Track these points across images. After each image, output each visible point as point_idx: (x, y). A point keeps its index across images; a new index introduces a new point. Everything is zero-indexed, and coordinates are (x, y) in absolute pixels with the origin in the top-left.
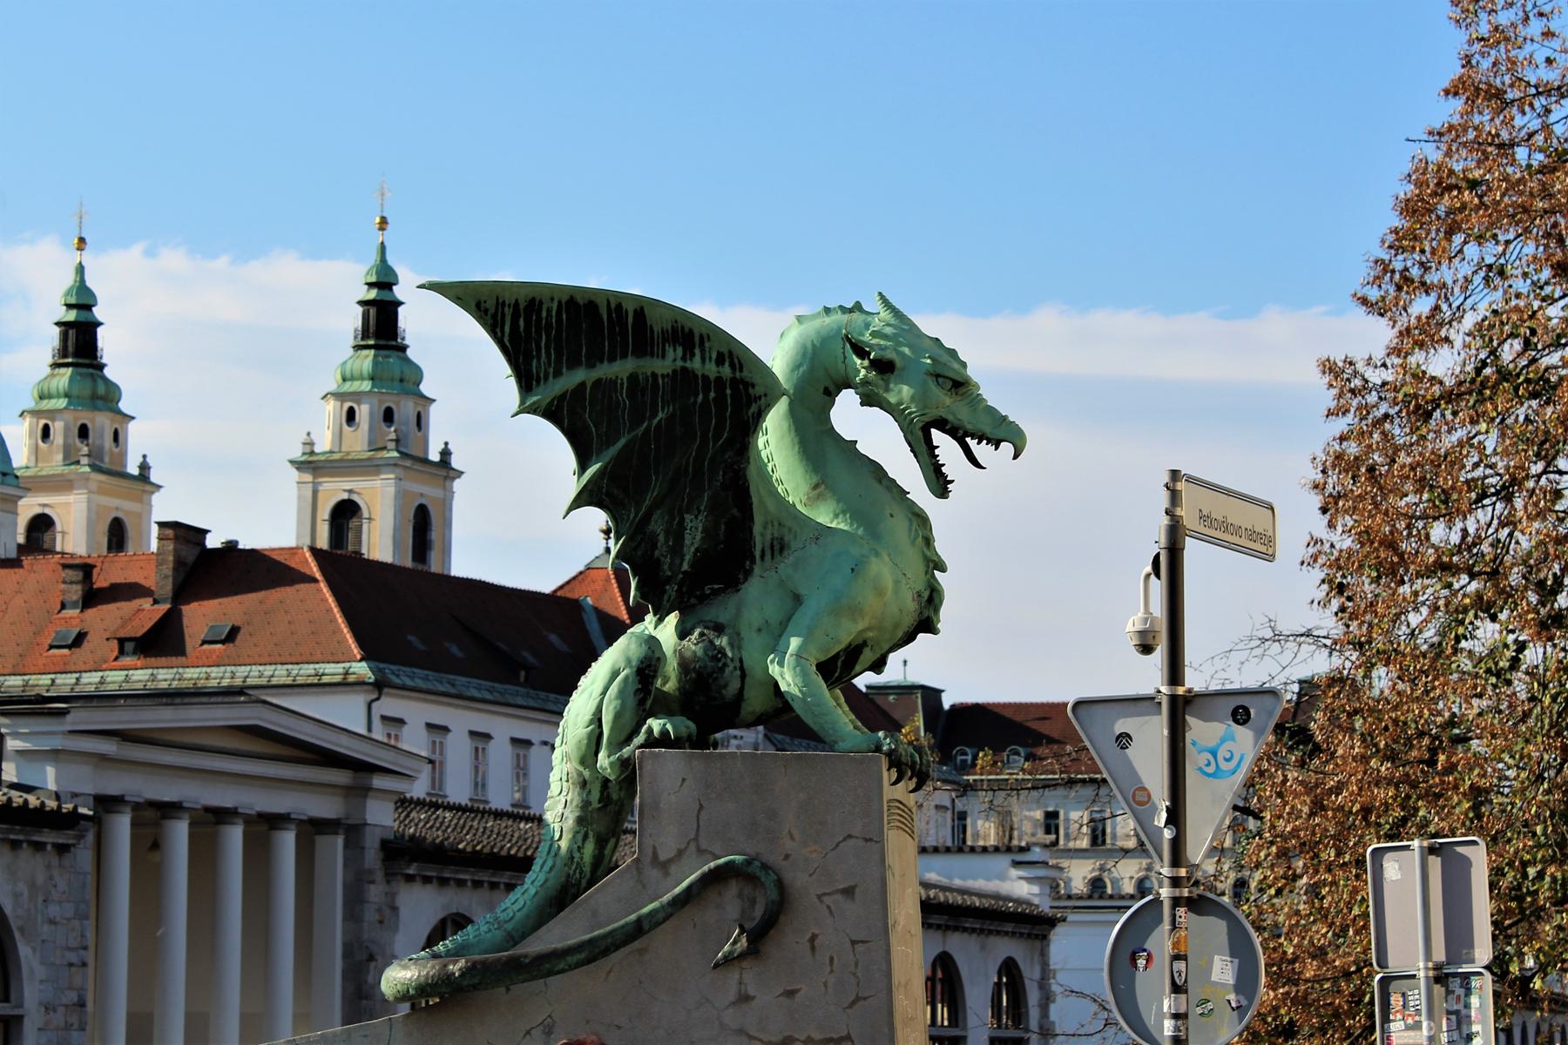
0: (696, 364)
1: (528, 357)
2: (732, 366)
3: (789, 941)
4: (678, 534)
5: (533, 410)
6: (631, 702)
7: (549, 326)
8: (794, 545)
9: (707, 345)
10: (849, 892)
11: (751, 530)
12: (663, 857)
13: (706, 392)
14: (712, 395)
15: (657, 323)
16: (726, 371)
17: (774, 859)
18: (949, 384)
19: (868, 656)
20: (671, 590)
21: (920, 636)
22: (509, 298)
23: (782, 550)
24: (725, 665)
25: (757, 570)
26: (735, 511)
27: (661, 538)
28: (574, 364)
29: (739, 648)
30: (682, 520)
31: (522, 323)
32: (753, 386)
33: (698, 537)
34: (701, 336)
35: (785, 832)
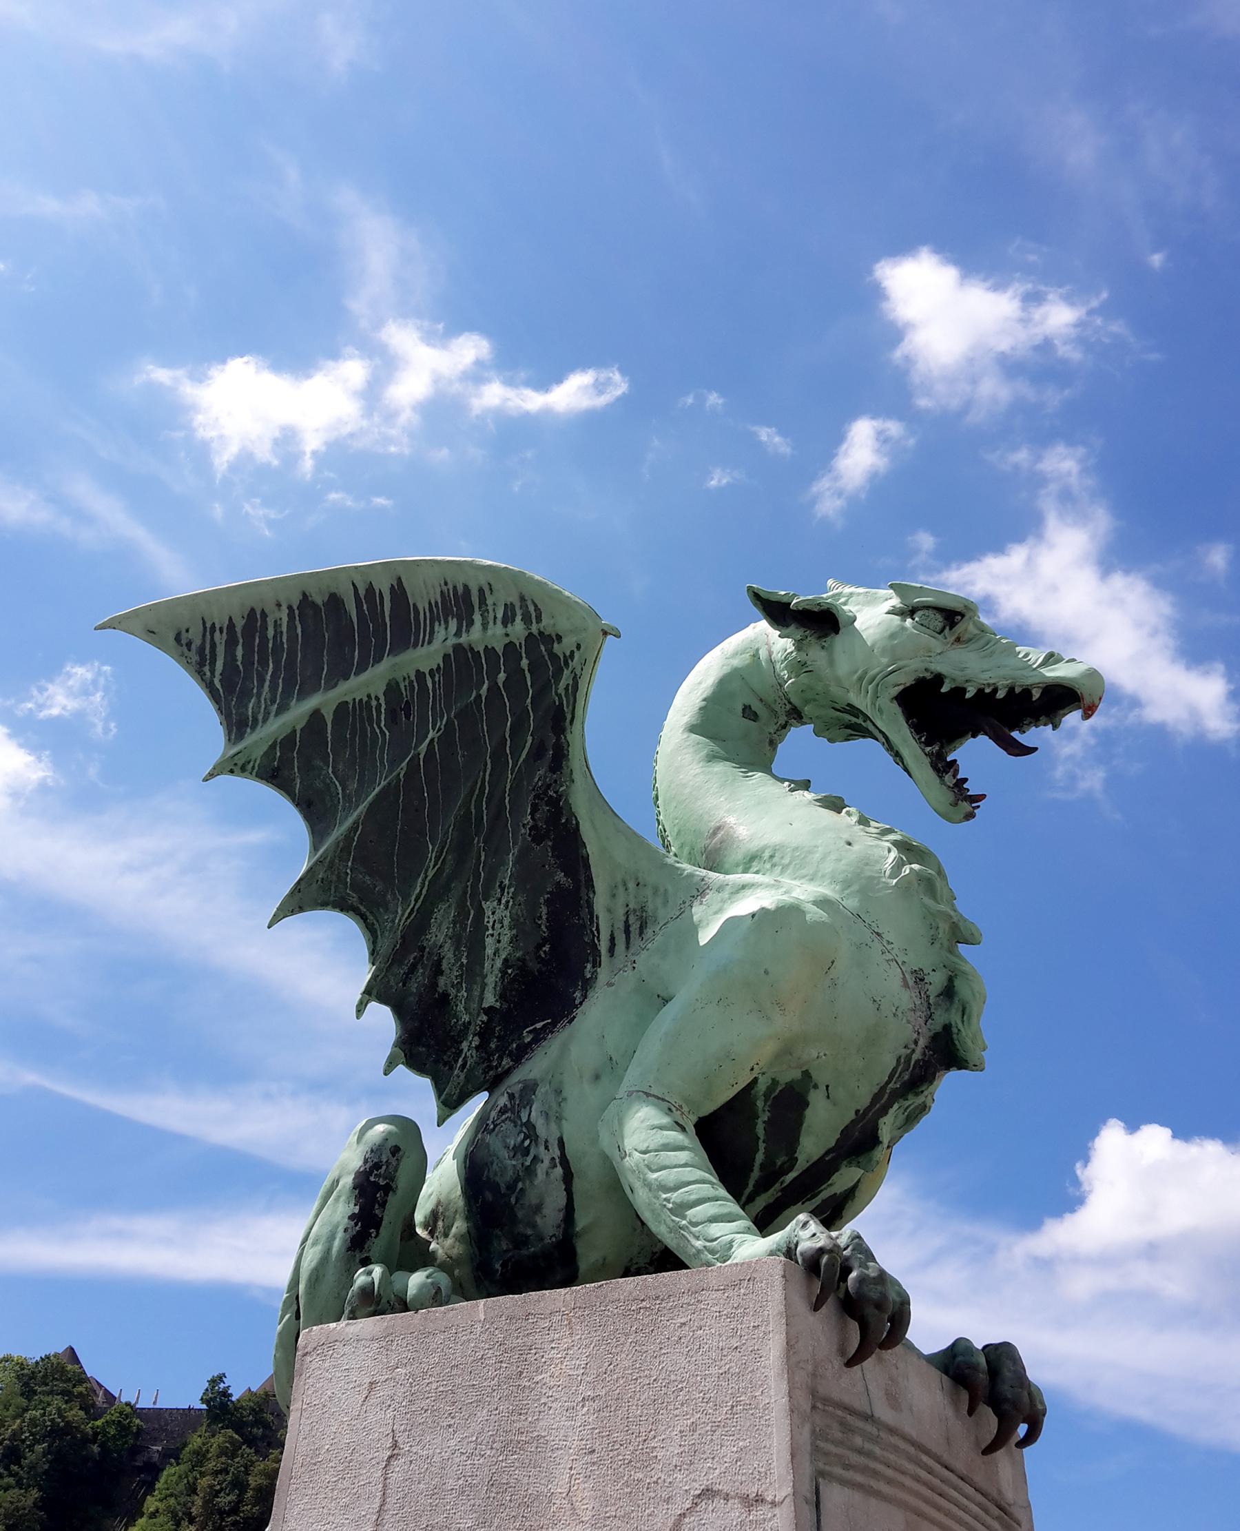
0: (475, 636)
1: (245, 695)
2: (527, 619)
8: (662, 914)
9: (490, 601)
11: (590, 905)
14: (502, 676)
15: (421, 596)
18: (937, 621)
20: (469, 1045)
22: (221, 620)
24: (536, 1159)
25: (603, 974)
26: (560, 876)
27: (448, 953)
29: (559, 1119)
30: (480, 913)
31: (239, 652)
32: (559, 638)
33: (505, 940)
34: (481, 591)
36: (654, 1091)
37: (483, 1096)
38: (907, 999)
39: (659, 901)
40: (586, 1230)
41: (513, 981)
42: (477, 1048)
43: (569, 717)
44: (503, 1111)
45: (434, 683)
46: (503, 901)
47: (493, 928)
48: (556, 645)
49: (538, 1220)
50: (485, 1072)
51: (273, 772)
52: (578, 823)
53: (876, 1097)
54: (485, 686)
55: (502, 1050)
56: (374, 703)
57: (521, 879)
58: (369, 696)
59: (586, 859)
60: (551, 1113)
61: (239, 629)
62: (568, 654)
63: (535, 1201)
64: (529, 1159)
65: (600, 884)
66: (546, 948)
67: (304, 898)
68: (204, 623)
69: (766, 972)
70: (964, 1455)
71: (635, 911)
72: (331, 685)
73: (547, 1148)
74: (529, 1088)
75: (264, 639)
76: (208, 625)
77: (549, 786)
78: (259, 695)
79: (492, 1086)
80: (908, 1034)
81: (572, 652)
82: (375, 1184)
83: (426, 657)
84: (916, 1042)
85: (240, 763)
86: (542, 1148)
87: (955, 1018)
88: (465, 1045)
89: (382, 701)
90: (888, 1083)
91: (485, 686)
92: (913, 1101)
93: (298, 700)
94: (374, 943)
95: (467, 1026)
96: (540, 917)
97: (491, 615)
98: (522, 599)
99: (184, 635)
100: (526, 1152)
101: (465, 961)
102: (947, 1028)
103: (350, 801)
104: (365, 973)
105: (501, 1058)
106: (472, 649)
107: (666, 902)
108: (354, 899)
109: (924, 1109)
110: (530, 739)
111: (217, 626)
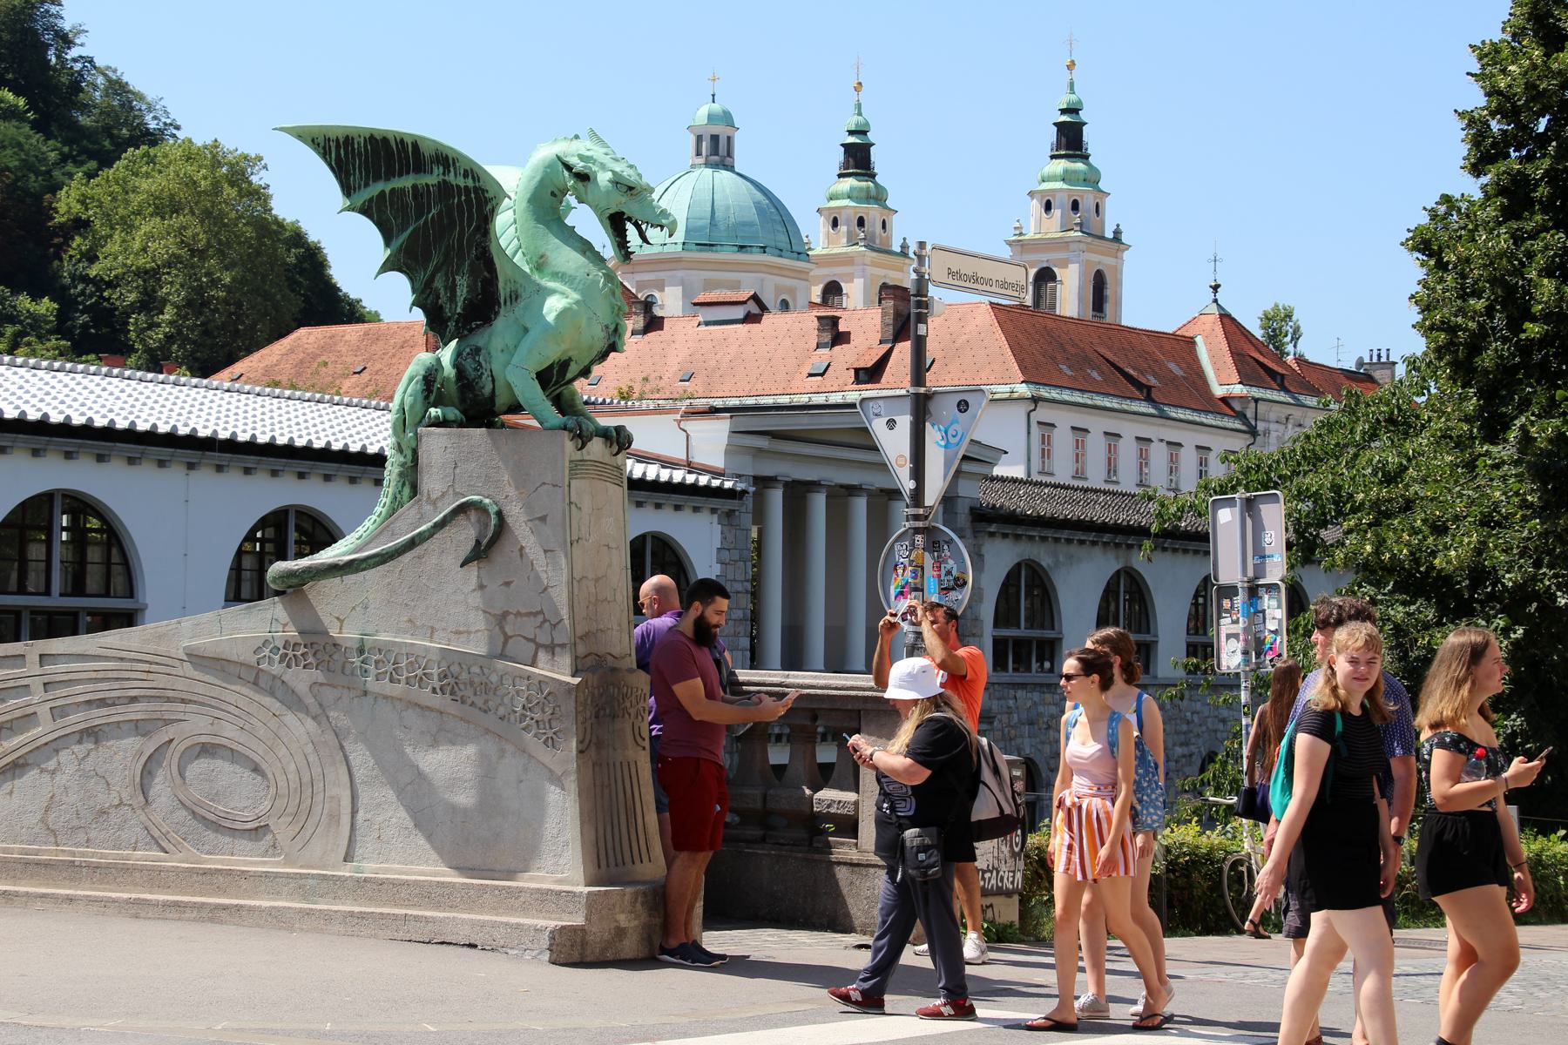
0: (451, 178)
1: (348, 174)
3: (505, 550)
5: (350, 209)
6: (420, 398)
7: (360, 154)
12: (434, 497)
15: (427, 151)
16: (470, 183)
19: (573, 369)
20: (451, 325)
21: (612, 355)
25: (502, 311)
27: (442, 292)
28: (377, 178)
51: (365, 211)
55: (464, 327)
67: (388, 266)
70: (607, 459)
72: (387, 179)
74: (477, 351)
83: (431, 179)
104: (410, 298)
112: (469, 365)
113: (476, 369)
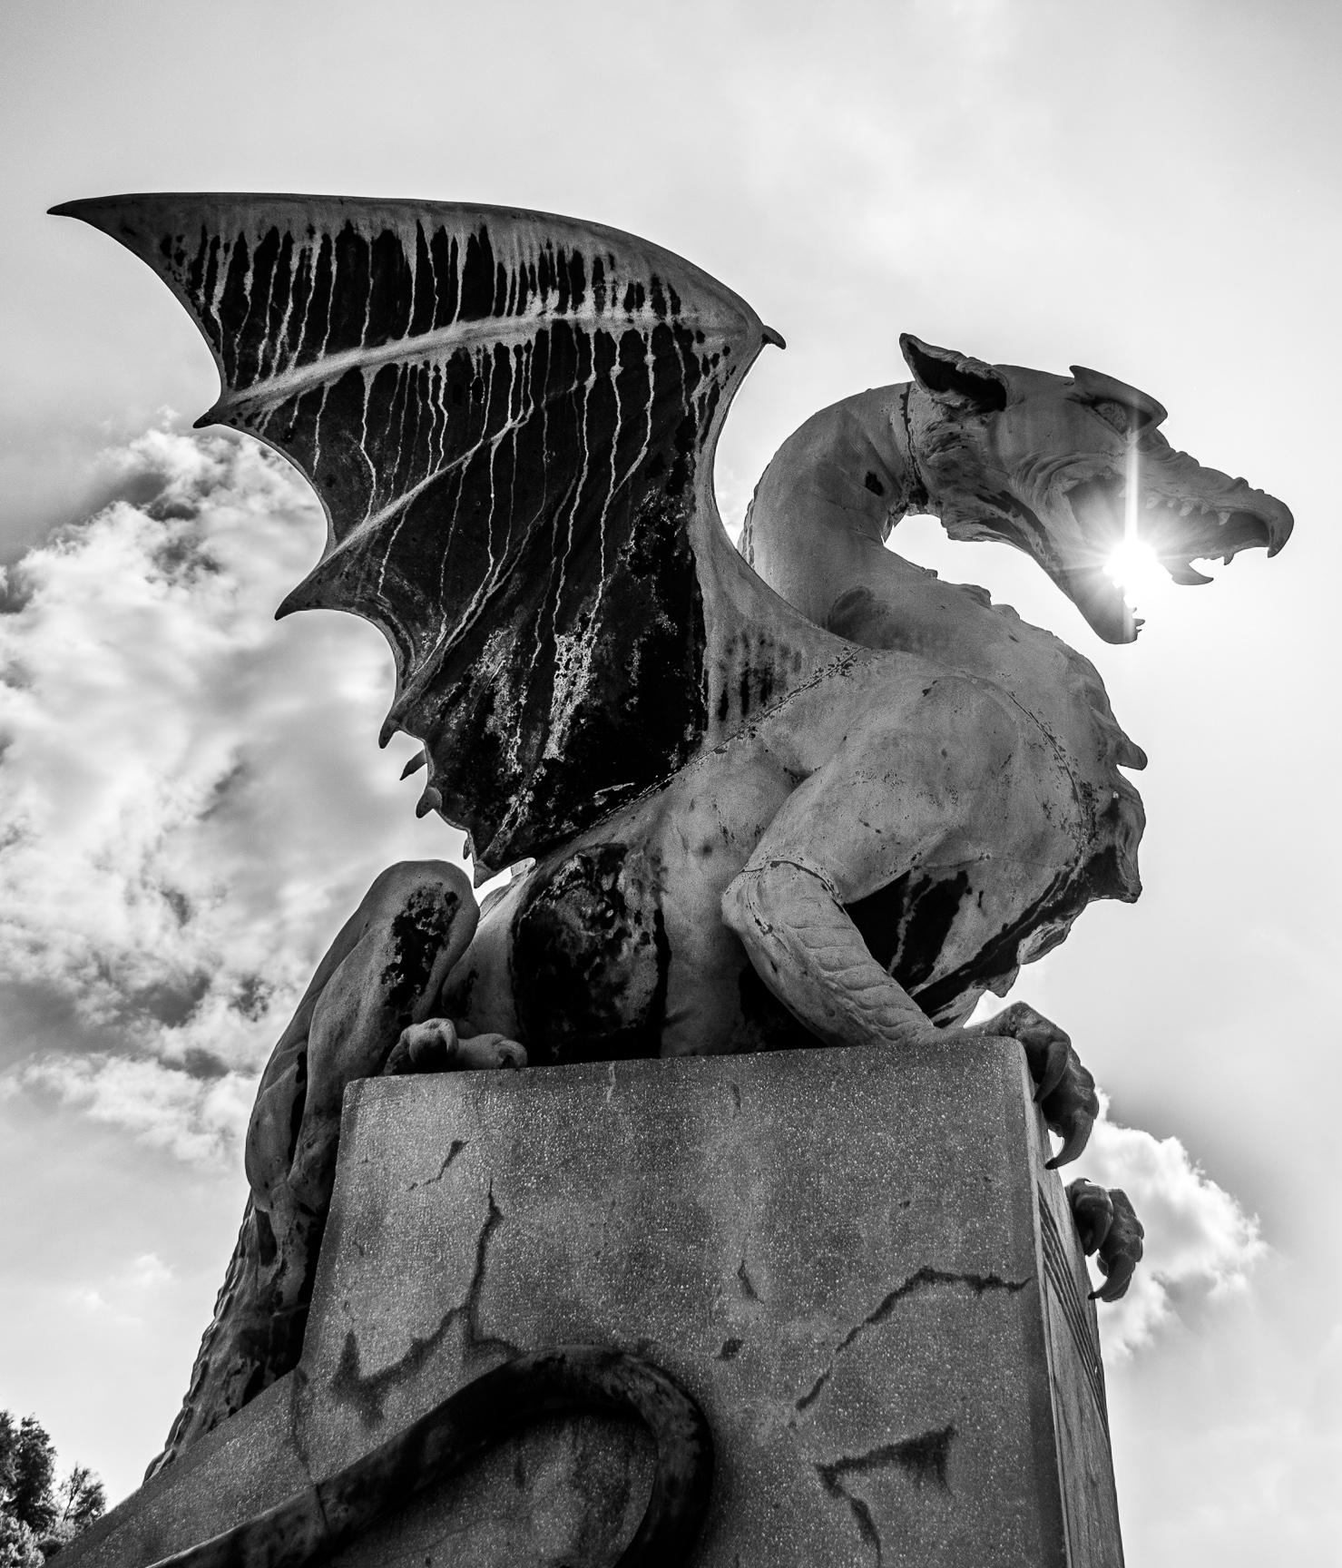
1: (253, 335)
2: (659, 307)
4: (536, 679)
7: (302, 284)
9: (609, 277)
10: (925, 1456)
13: (604, 365)
14: (616, 369)
15: (513, 253)
17: (695, 1353)
23: (765, 695)
24: (623, 933)
25: (709, 740)
26: (663, 619)
29: (657, 890)
30: (550, 648)
31: (249, 280)
34: (598, 263)
35: (730, 1275)
36: (806, 864)
37: (532, 861)
38: (1073, 812)
39: (789, 665)
40: (678, 1018)
41: (584, 733)
42: (530, 804)
43: (700, 432)
44: (574, 875)
45: (519, 363)
46: (586, 637)
47: (567, 667)
48: (695, 345)
49: (618, 1003)
50: (538, 834)
52: (694, 560)
53: (1027, 914)
54: (593, 377)
55: (562, 812)
56: (432, 374)
57: (611, 616)
58: (427, 364)
59: (699, 602)
60: (646, 883)
61: (251, 251)
62: (710, 357)
63: (613, 976)
64: (610, 934)
65: (714, 638)
66: (634, 700)
68: (204, 235)
69: (944, 753)
71: (756, 671)
72: (375, 340)
73: (638, 920)
74: (613, 857)
75: (284, 270)
76: (210, 238)
77: (662, 511)
78: (273, 337)
79: (541, 853)
80: (1072, 849)
81: (716, 357)
82: (423, 933)
83: (515, 329)
84: (1076, 861)
85: (246, 414)
86: (630, 922)
87: (1119, 842)
88: (513, 799)
89: (443, 373)
90: (1042, 899)
91: (593, 377)
92: (1058, 925)
93: (329, 351)
94: (407, 662)
95: (517, 779)
96: (631, 664)
97: (609, 293)
98: (655, 281)
99: (174, 243)
100: (608, 923)
101: (523, 702)
102: (1111, 850)
103: (387, 489)
105: (559, 822)
106: (578, 330)
107: (797, 668)
108: (386, 605)
109: (1060, 937)
110: (644, 450)
111: (223, 242)
112: (575, 913)
113: (598, 921)
